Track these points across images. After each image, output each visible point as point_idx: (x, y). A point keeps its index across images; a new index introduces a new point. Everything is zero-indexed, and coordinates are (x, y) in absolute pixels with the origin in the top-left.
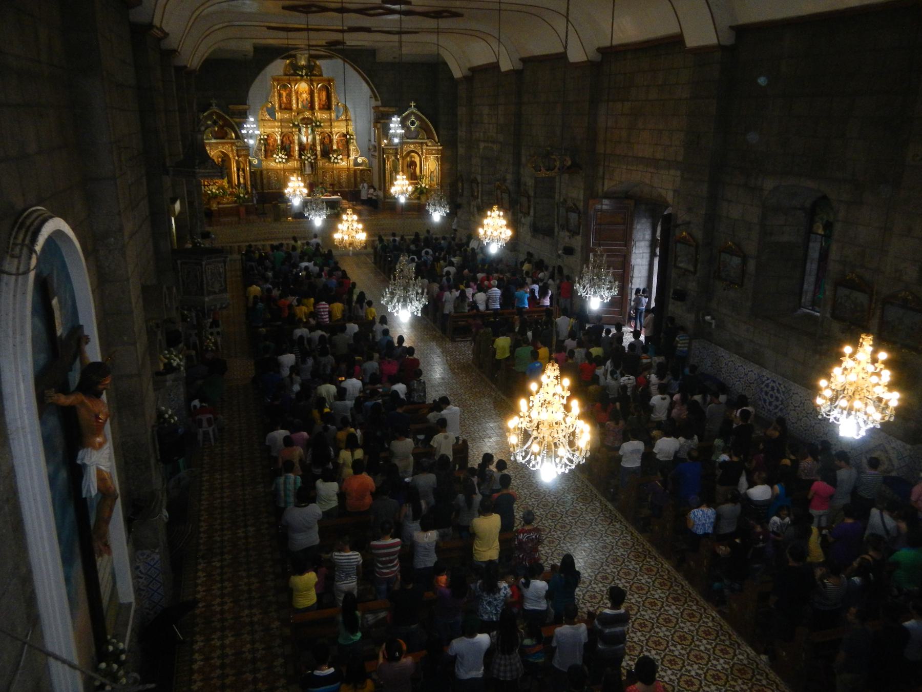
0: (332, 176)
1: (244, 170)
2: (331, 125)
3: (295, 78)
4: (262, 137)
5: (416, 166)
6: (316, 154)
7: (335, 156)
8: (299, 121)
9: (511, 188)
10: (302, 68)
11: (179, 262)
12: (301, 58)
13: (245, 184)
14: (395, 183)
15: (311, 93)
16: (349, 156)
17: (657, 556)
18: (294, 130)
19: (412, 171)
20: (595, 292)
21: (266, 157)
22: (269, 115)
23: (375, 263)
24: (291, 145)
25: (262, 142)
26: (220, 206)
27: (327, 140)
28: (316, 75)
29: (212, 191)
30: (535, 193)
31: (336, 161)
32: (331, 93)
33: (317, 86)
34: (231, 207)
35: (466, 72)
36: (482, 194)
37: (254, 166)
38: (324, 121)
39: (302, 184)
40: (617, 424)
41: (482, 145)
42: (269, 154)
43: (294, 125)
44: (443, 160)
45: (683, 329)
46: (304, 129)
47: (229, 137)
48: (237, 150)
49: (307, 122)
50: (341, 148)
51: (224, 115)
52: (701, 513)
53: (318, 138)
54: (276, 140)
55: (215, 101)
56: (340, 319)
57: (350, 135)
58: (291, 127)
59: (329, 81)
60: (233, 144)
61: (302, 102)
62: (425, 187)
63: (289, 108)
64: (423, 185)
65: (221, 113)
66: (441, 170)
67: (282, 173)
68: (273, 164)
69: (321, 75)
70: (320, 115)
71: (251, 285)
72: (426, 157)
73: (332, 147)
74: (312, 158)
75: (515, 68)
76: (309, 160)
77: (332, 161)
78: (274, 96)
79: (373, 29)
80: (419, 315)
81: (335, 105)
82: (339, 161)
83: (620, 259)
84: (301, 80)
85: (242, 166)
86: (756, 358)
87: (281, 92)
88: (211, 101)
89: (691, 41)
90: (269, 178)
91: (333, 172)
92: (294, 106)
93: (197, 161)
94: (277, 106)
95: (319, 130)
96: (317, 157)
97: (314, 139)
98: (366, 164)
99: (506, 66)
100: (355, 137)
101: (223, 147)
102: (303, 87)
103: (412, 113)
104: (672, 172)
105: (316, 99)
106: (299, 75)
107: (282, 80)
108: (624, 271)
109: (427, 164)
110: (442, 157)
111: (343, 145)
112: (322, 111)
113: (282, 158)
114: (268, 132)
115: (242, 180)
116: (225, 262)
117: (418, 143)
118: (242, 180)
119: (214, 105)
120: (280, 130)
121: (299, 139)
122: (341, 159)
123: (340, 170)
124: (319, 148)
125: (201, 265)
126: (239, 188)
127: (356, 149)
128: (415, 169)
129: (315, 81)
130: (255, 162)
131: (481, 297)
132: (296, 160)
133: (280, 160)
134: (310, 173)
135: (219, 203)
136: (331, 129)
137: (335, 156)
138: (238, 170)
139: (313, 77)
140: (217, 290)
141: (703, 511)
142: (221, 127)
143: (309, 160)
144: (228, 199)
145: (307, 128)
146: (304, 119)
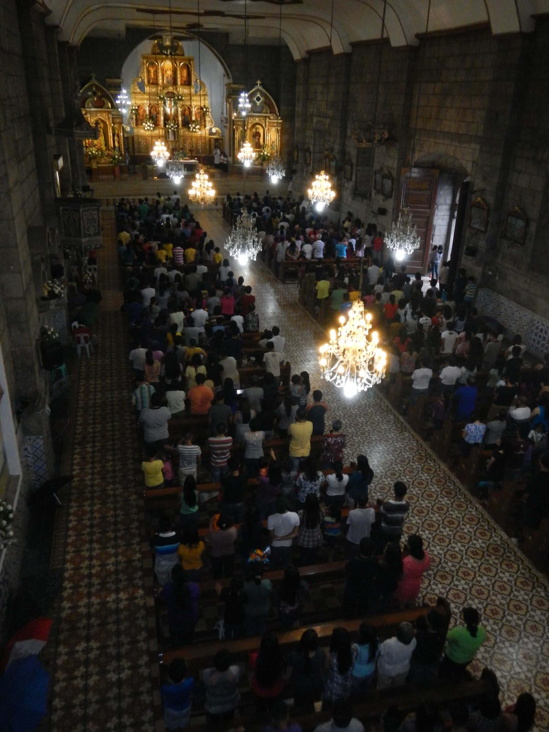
0: (191, 143)
2: (191, 99)
3: (161, 56)
4: (134, 108)
5: (260, 136)
6: (178, 124)
7: (194, 126)
8: (164, 95)
9: (337, 156)
10: (166, 48)
11: (61, 208)
12: (166, 39)
13: (119, 147)
15: (175, 71)
16: (205, 126)
17: (436, 459)
18: (160, 102)
19: (257, 140)
20: (400, 246)
21: (137, 125)
22: (140, 88)
23: (224, 217)
25: (134, 112)
26: (99, 165)
27: (187, 112)
28: (178, 55)
29: (92, 152)
30: (357, 162)
31: (194, 130)
33: (180, 64)
34: (109, 166)
35: (304, 55)
36: (313, 162)
37: (127, 132)
38: (185, 95)
39: (165, 148)
40: (411, 354)
41: (315, 119)
42: (139, 122)
43: (160, 98)
44: (283, 132)
45: (472, 279)
47: (106, 106)
48: (113, 118)
49: (171, 95)
51: (102, 87)
52: (474, 427)
53: (180, 110)
54: (145, 111)
55: (95, 75)
56: (193, 262)
57: (206, 108)
58: (158, 100)
59: (190, 60)
60: (109, 113)
61: (167, 78)
63: (156, 84)
64: (266, 153)
65: (100, 85)
66: (281, 141)
67: (150, 139)
68: (142, 131)
69: (183, 55)
70: (182, 90)
71: (122, 231)
72: (268, 129)
73: (191, 118)
75: (346, 52)
77: (191, 130)
78: (143, 72)
79: (226, 13)
80: (255, 259)
82: (197, 130)
83: (425, 220)
85: (117, 132)
86: (530, 305)
87: (150, 69)
89: (497, 29)
90: (139, 143)
91: (191, 140)
92: (160, 81)
93: (75, 123)
94: (146, 81)
96: (178, 126)
98: (219, 133)
99: (337, 50)
100: (210, 110)
101: (101, 115)
102: (168, 64)
103: (258, 90)
104: (473, 145)
105: (179, 76)
106: (164, 54)
108: (427, 230)
110: (282, 130)
111: (201, 117)
112: (184, 87)
115: (117, 144)
116: (98, 210)
117: (263, 116)
118: (117, 144)
119: (93, 78)
121: (164, 110)
122: (199, 129)
123: (197, 138)
124: (180, 119)
125: (78, 211)
126: (114, 150)
128: (259, 139)
129: (178, 59)
130: (128, 129)
131: (308, 248)
132: (162, 129)
133: (149, 128)
134: (173, 139)
135: (98, 163)
138: (114, 135)
139: (176, 57)
140: (92, 233)
141: (476, 426)
142: (100, 98)
143: (172, 129)
144: (105, 160)
145: (170, 100)
146: (168, 93)
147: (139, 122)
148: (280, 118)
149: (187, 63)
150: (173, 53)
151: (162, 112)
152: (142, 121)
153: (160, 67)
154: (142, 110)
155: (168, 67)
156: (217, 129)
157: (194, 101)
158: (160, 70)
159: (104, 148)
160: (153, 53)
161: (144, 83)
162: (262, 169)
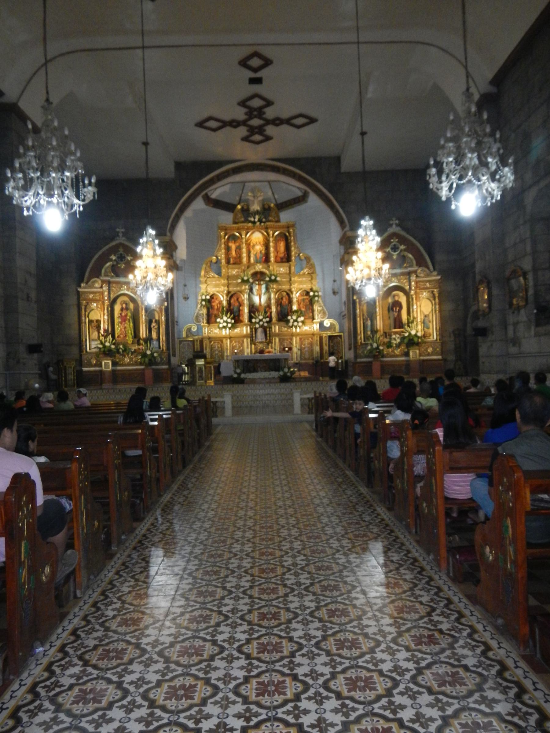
1: (158, 322)
2: (290, 280)
4: (204, 297)
5: (401, 307)
8: (249, 276)
14: (354, 258)
15: (267, 246)
16: (313, 318)
19: (396, 314)
21: (209, 322)
23: (316, 430)
24: (241, 308)
25: (204, 303)
26: (119, 368)
27: (285, 301)
29: (104, 346)
31: (296, 324)
32: (291, 242)
42: (213, 319)
43: (243, 281)
46: (257, 287)
49: (259, 276)
50: (303, 309)
53: (272, 296)
54: (221, 302)
58: (238, 285)
61: (255, 255)
62: (416, 335)
63: (238, 261)
64: (413, 332)
66: (440, 311)
68: (217, 331)
69: (278, 221)
74: (264, 320)
76: (261, 323)
77: (291, 324)
81: (295, 257)
82: (300, 324)
84: (254, 227)
87: (230, 244)
88: (118, 230)
92: (245, 260)
94: (223, 261)
95: (275, 286)
96: (271, 320)
97: (269, 299)
102: (257, 237)
105: (272, 249)
106: (250, 222)
107: (232, 229)
109: (418, 304)
110: (440, 293)
111: (306, 306)
112: (279, 264)
113: (227, 323)
114: (212, 293)
118: (154, 335)
119: (121, 235)
120: (226, 288)
121: (250, 299)
122: (303, 322)
124: (274, 309)
127: (323, 310)
128: (400, 311)
133: (225, 324)
135: (114, 364)
136: (291, 285)
137: (294, 317)
138: (150, 322)
139: (268, 223)
143: (261, 323)
145: (260, 285)
146: (255, 274)
147: (210, 319)
148: (435, 273)
149: (284, 231)
150: (264, 220)
151: (246, 302)
152: (217, 316)
153: (244, 240)
154: (217, 302)
155: (257, 240)
156: (332, 321)
157: (295, 282)
158: (244, 245)
159: (130, 339)
160: (235, 223)
161: (221, 263)
162: (407, 361)
